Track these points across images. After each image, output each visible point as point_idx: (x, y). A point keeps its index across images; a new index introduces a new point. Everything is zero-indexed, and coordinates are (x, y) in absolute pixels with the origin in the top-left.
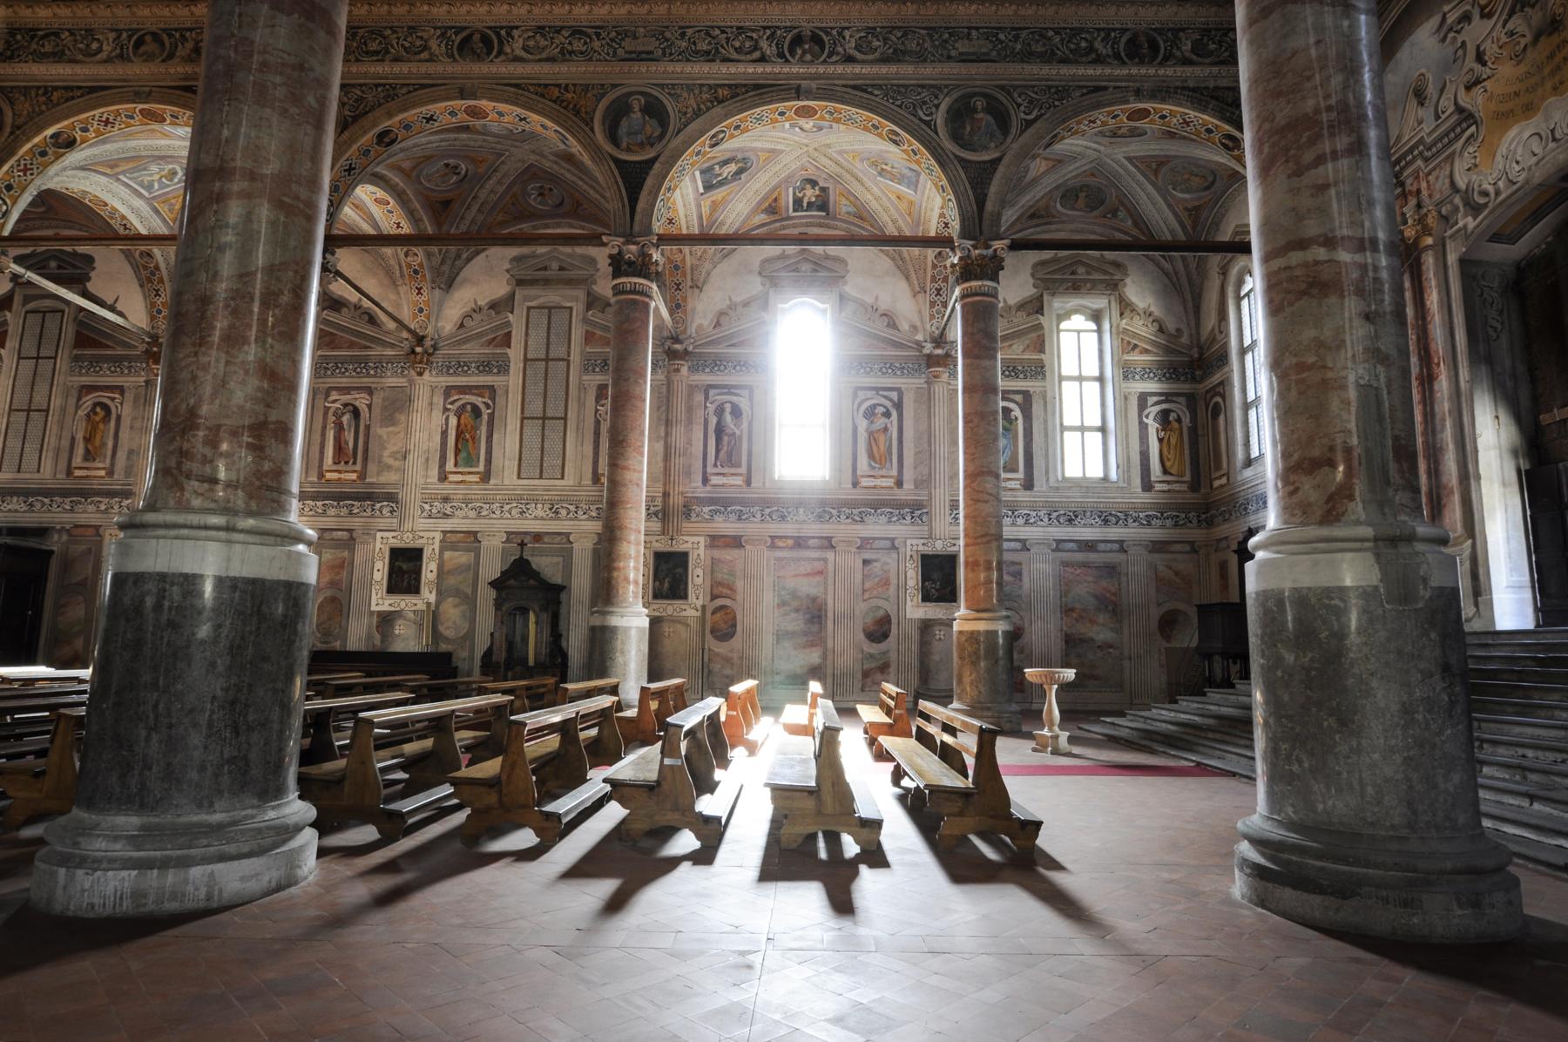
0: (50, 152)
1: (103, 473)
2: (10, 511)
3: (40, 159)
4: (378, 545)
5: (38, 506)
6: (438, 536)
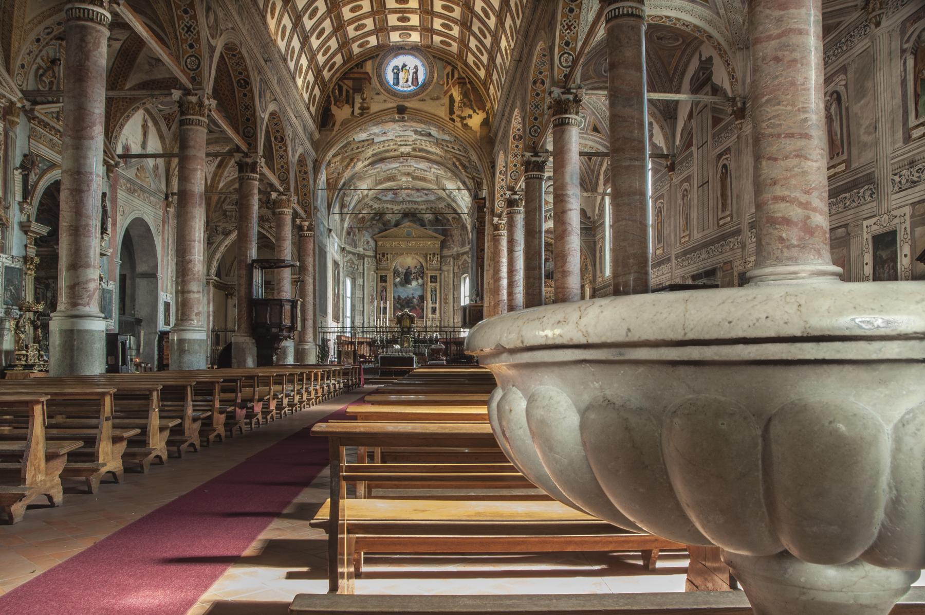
0: (573, 7)
1: (728, 219)
2: (704, 259)
3: (572, 15)
4: (865, 236)
5: (711, 251)
6: (907, 210)
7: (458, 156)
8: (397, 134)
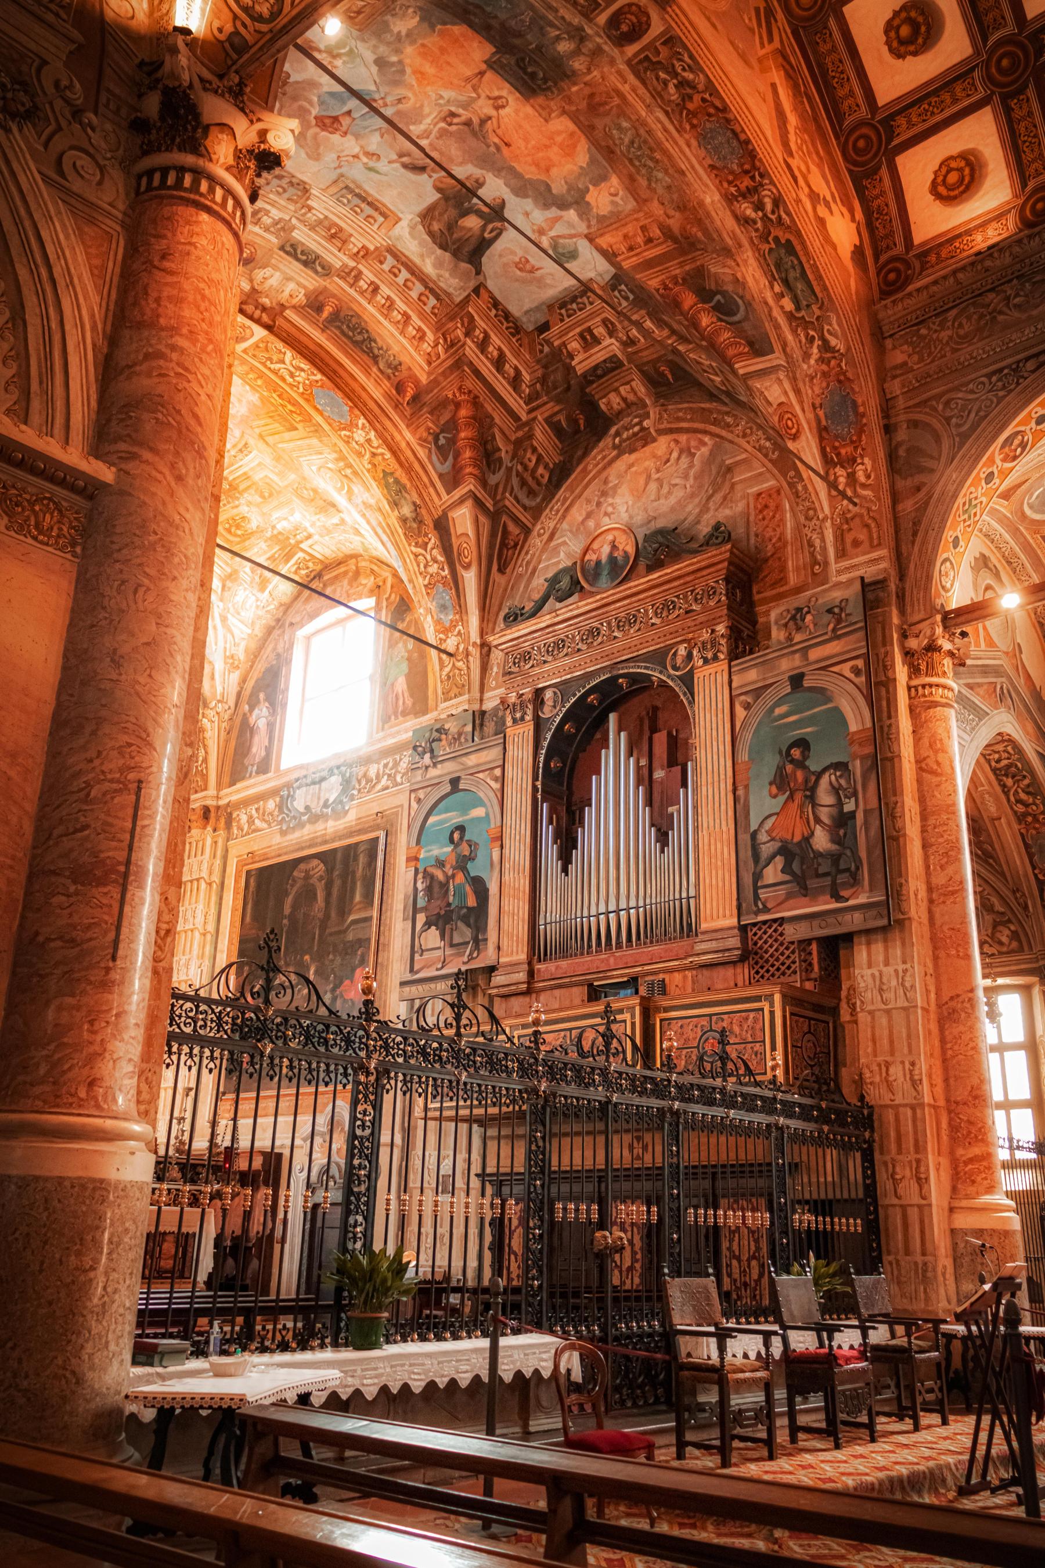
7: (490, 407)
8: (357, 173)
